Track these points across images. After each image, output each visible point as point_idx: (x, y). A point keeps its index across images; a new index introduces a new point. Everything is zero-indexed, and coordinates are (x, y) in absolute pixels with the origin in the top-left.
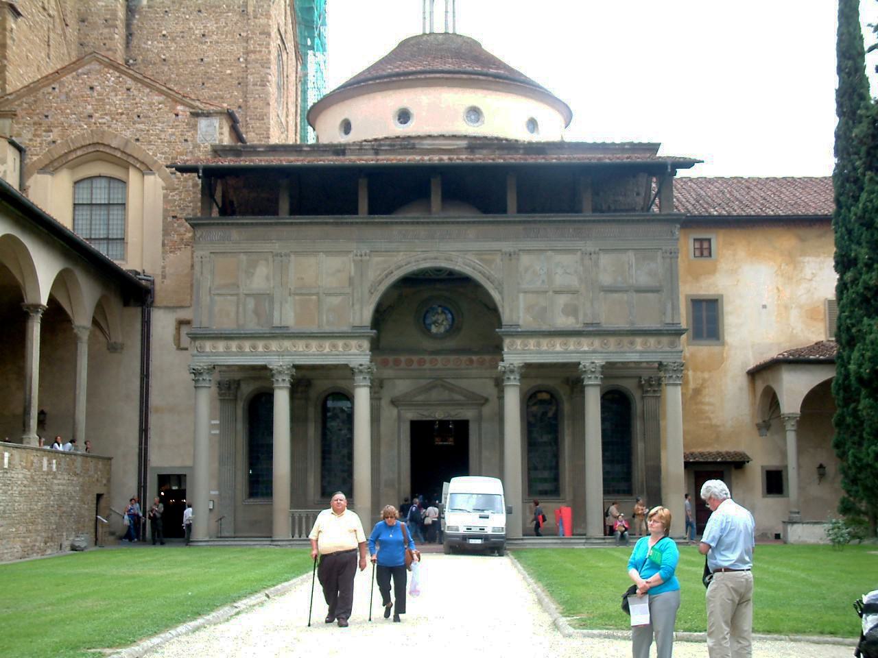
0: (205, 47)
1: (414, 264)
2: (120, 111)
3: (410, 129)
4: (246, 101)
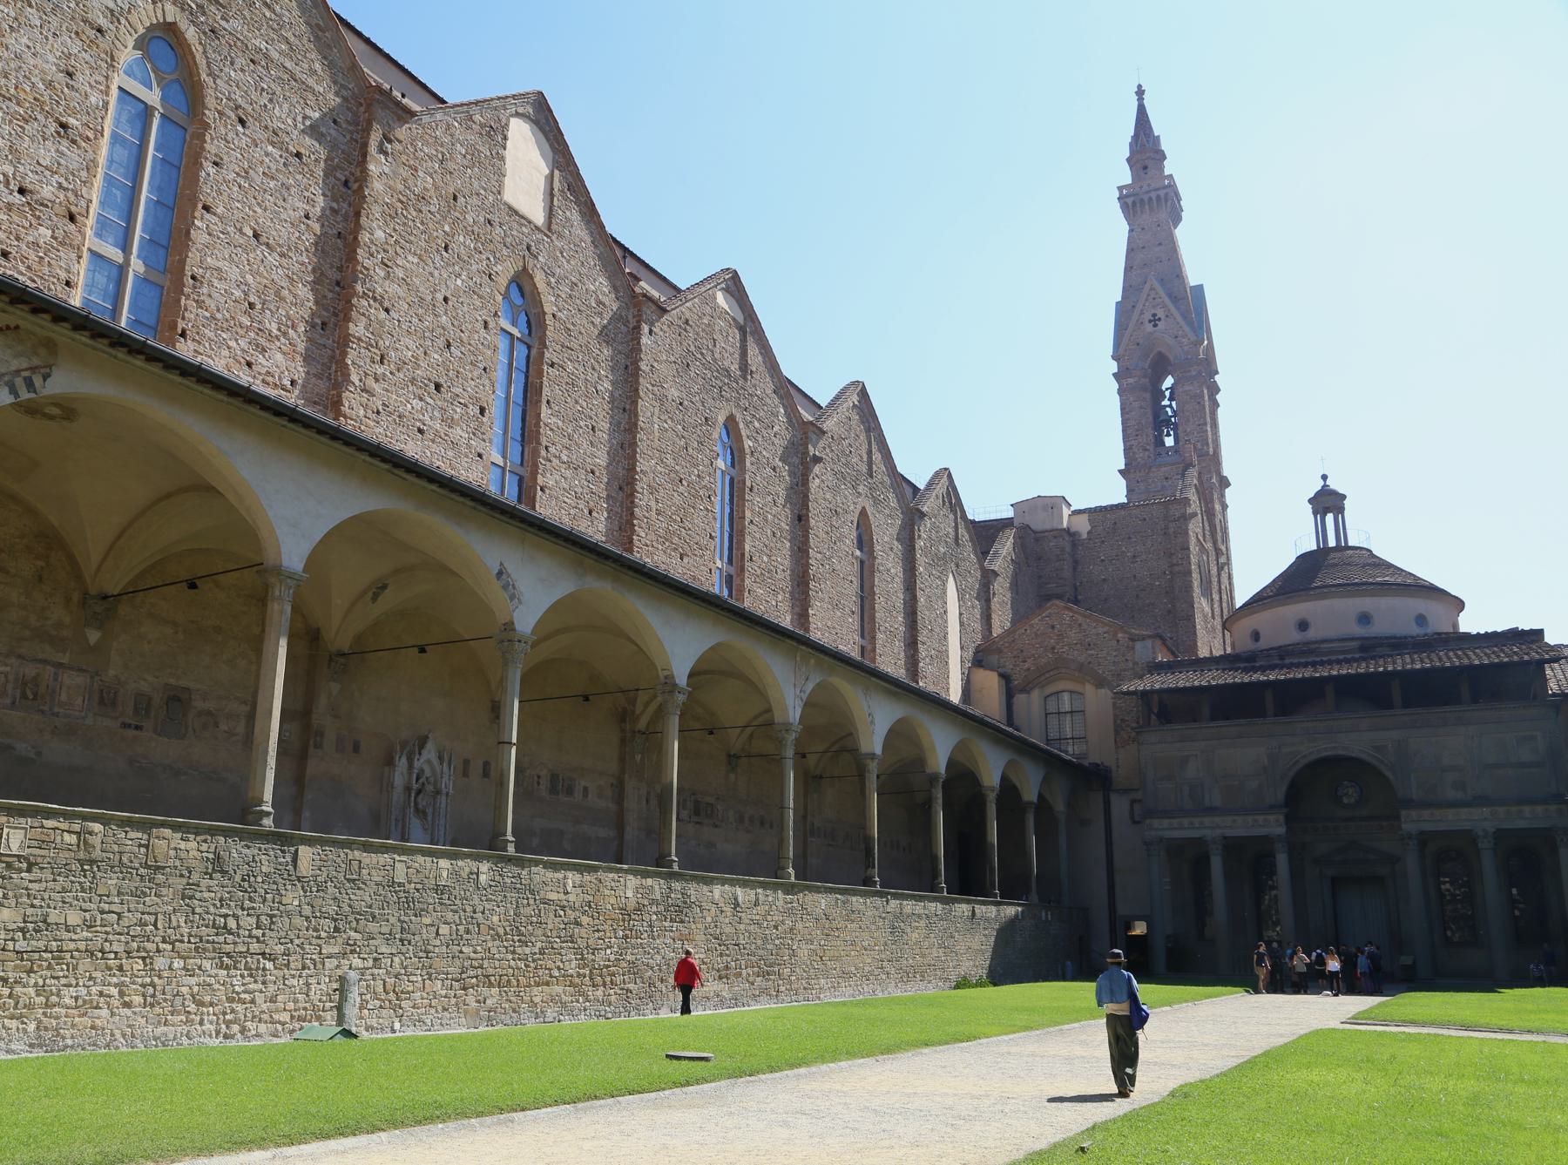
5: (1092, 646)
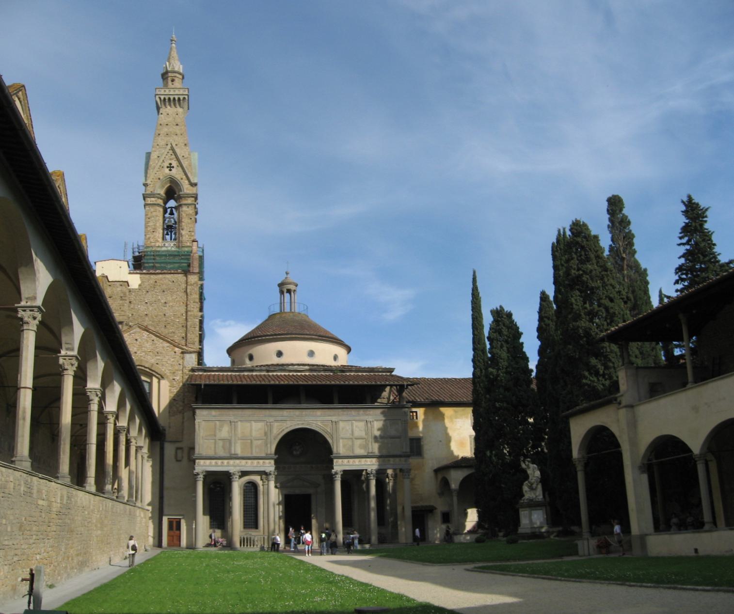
0: (166, 308)
2: (149, 350)
4: (186, 335)
5: (159, 354)
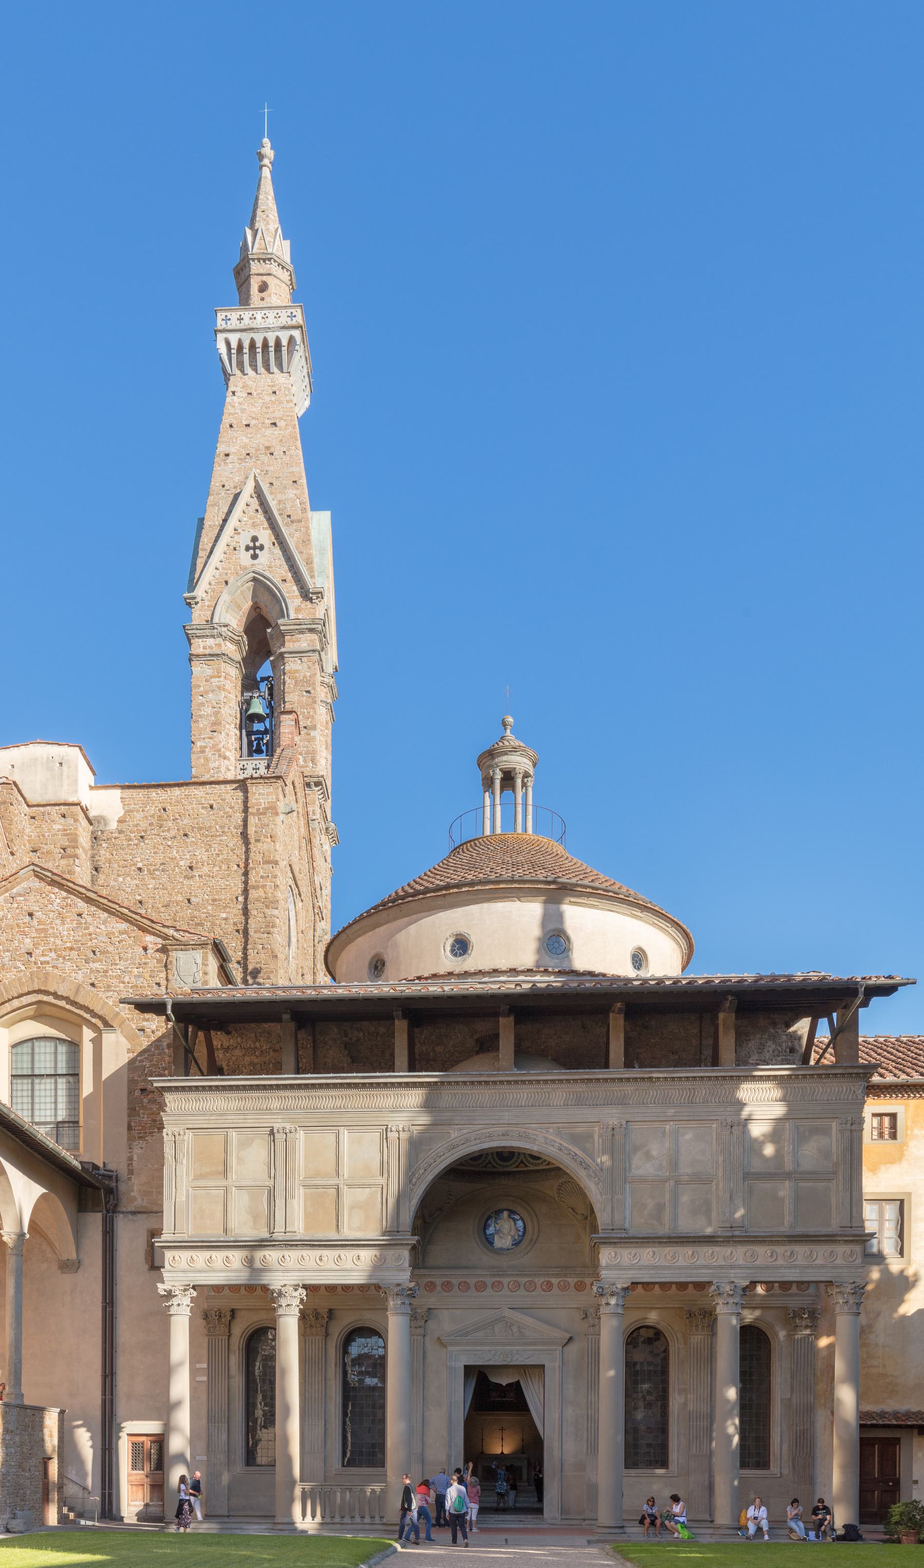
1: (473, 1143)
3: (470, 963)
